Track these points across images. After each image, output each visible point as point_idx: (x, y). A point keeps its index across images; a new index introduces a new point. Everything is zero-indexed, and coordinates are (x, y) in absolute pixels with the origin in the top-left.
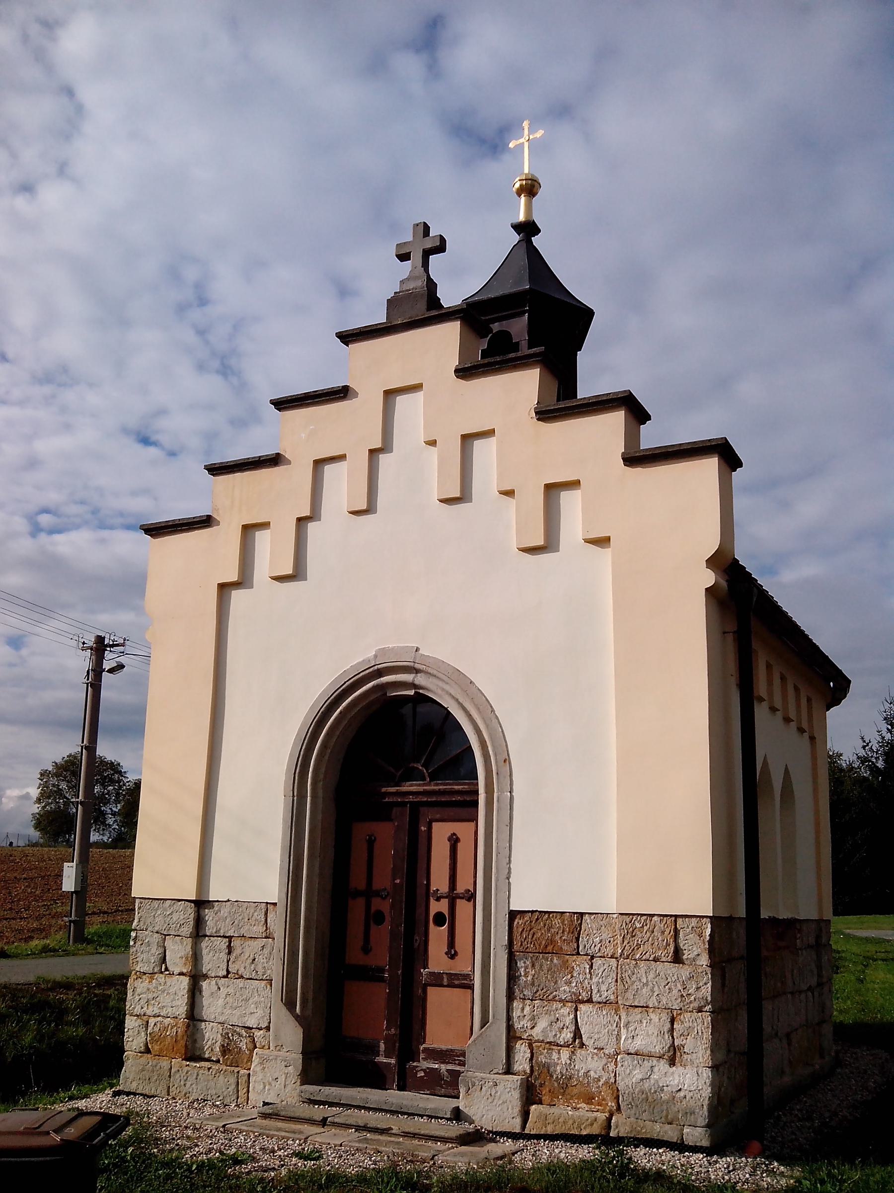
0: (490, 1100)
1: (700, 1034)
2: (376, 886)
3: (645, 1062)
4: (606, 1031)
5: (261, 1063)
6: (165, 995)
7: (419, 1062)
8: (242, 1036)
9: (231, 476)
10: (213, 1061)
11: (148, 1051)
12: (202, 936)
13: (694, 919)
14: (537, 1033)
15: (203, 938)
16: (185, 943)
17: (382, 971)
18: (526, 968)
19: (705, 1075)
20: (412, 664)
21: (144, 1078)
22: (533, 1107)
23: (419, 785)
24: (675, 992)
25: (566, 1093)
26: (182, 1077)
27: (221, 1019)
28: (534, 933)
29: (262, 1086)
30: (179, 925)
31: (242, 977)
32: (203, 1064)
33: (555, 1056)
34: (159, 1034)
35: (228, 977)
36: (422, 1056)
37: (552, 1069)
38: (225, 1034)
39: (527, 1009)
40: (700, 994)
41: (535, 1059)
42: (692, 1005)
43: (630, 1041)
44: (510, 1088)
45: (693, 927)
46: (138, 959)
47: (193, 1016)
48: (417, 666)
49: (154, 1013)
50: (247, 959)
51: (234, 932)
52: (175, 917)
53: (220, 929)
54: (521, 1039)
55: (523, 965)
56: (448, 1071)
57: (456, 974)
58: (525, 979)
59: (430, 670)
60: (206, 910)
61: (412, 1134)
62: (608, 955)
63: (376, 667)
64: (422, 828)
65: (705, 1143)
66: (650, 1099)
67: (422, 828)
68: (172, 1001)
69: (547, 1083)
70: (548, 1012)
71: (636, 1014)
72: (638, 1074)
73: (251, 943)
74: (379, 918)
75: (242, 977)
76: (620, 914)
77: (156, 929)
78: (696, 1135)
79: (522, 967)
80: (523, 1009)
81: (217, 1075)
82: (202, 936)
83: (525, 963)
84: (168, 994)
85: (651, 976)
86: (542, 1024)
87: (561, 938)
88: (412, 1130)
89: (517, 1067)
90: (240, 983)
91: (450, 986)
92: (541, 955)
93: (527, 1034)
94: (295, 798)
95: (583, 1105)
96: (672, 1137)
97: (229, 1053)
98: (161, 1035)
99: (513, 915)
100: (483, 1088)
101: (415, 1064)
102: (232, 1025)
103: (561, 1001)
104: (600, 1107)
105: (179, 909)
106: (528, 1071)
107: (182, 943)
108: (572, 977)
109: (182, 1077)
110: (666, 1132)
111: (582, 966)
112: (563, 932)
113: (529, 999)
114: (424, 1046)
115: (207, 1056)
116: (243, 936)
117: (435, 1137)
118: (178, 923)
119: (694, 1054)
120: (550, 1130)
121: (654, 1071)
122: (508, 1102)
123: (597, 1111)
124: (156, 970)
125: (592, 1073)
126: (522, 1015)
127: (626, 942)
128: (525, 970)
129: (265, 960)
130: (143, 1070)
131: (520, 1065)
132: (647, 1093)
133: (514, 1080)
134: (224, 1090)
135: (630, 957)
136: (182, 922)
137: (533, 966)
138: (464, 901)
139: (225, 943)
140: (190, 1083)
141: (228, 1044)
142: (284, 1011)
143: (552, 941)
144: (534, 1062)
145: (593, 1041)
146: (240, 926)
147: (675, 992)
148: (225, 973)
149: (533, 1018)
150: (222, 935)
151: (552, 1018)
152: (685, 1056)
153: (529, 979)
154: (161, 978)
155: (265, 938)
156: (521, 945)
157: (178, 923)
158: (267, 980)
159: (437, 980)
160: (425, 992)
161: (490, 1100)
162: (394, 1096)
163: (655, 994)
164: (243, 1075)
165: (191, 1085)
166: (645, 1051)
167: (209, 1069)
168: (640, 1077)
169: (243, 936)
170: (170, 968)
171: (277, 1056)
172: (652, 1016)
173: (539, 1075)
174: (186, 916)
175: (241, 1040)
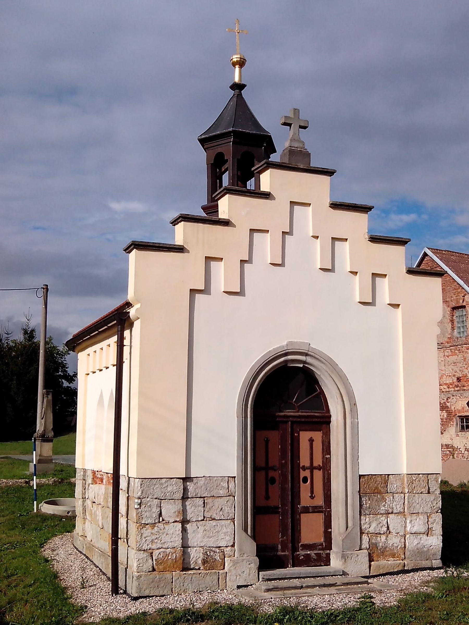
0: (355, 563)
1: (438, 522)
2: (271, 464)
3: (418, 536)
4: (400, 525)
5: (234, 565)
6: (165, 535)
7: (299, 551)
8: (216, 552)
9: (196, 224)
10: (196, 569)
11: (154, 570)
12: (186, 498)
13: (435, 475)
14: (371, 530)
15: (187, 499)
16: (177, 503)
17: (278, 508)
18: (366, 501)
19: (440, 538)
20: (307, 352)
21: (154, 586)
22: (372, 563)
23: (293, 412)
24: (429, 506)
25: (384, 554)
26: (181, 581)
27: (202, 545)
28: (369, 485)
29: (235, 577)
30: (173, 493)
31: (214, 519)
32: (190, 572)
33: (379, 539)
34: (163, 559)
35: (204, 520)
36: (300, 548)
37: (378, 545)
38: (205, 553)
39: (367, 519)
40: (438, 506)
41: (370, 541)
42: (434, 511)
43: (412, 528)
44: (364, 556)
45: (434, 478)
46: (142, 516)
47: (185, 546)
48: (309, 353)
49: (158, 547)
50: (217, 509)
51: (208, 494)
52: (169, 489)
53: (198, 493)
54: (364, 533)
55: (364, 499)
56: (315, 554)
57: (315, 506)
58: (366, 506)
59: (316, 356)
60: (188, 483)
61: (346, 583)
62: (399, 492)
63: (287, 351)
64: (296, 434)
65: (441, 565)
66: (420, 551)
67: (296, 434)
68: (171, 539)
69: (376, 552)
70: (376, 520)
71: (414, 517)
72: (416, 542)
73: (219, 499)
74: (273, 481)
75: (214, 519)
76: (407, 474)
77: (155, 497)
78: (437, 563)
79: (364, 500)
80: (365, 520)
81: (205, 577)
82: (186, 498)
83: (365, 498)
84: (167, 534)
85: (420, 499)
86: (374, 525)
87: (380, 486)
88: (345, 582)
89: (363, 547)
90: (214, 523)
91: (313, 512)
92: (372, 494)
93: (367, 531)
94: (243, 419)
95: (391, 559)
96: (429, 565)
97: (207, 563)
98: (164, 559)
99: (360, 476)
100: (352, 558)
101: (298, 553)
102: (209, 547)
103: (381, 514)
104: (398, 559)
105: (172, 483)
106: (368, 548)
107: (175, 503)
108: (386, 503)
109: (181, 581)
110: (427, 564)
111: (390, 498)
112: (382, 483)
113: (368, 515)
114: (301, 543)
115: (192, 567)
116: (213, 496)
117: (357, 583)
118: (172, 492)
119: (436, 531)
120: (381, 572)
121: (422, 539)
122: (364, 563)
123: (397, 560)
124: (156, 521)
125: (395, 545)
126: (365, 522)
127: (410, 486)
128: (366, 502)
129: (229, 508)
130: (152, 582)
131: (364, 545)
132: (419, 549)
133: (365, 553)
134: (210, 584)
135: (412, 492)
136: (175, 491)
137: (369, 500)
138: (317, 470)
139: (202, 501)
140: (187, 584)
141: (207, 558)
142: (244, 534)
143: (377, 488)
144: (370, 543)
145: (395, 530)
146: (211, 491)
147: (429, 506)
148: (203, 518)
149: (370, 524)
150: (199, 496)
151: (378, 522)
152: (433, 532)
153: (367, 505)
154: (160, 525)
155: (228, 496)
156: (364, 490)
157: (172, 492)
158: (230, 519)
159: (306, 510)
160: (300, 516)
161: (355, 563)
162: (290, 570)
163: (422, 507)
164: (222, 574)
165: (188, 584)
166: (418, 532)
167: (200, 574)
168: (417, 543)
169: (213, 496)
170: (166, 519)
171: (243, 560)
172: (421, 517)
173: (372, 548)
174: (177, 487)
175: (216, 555)
